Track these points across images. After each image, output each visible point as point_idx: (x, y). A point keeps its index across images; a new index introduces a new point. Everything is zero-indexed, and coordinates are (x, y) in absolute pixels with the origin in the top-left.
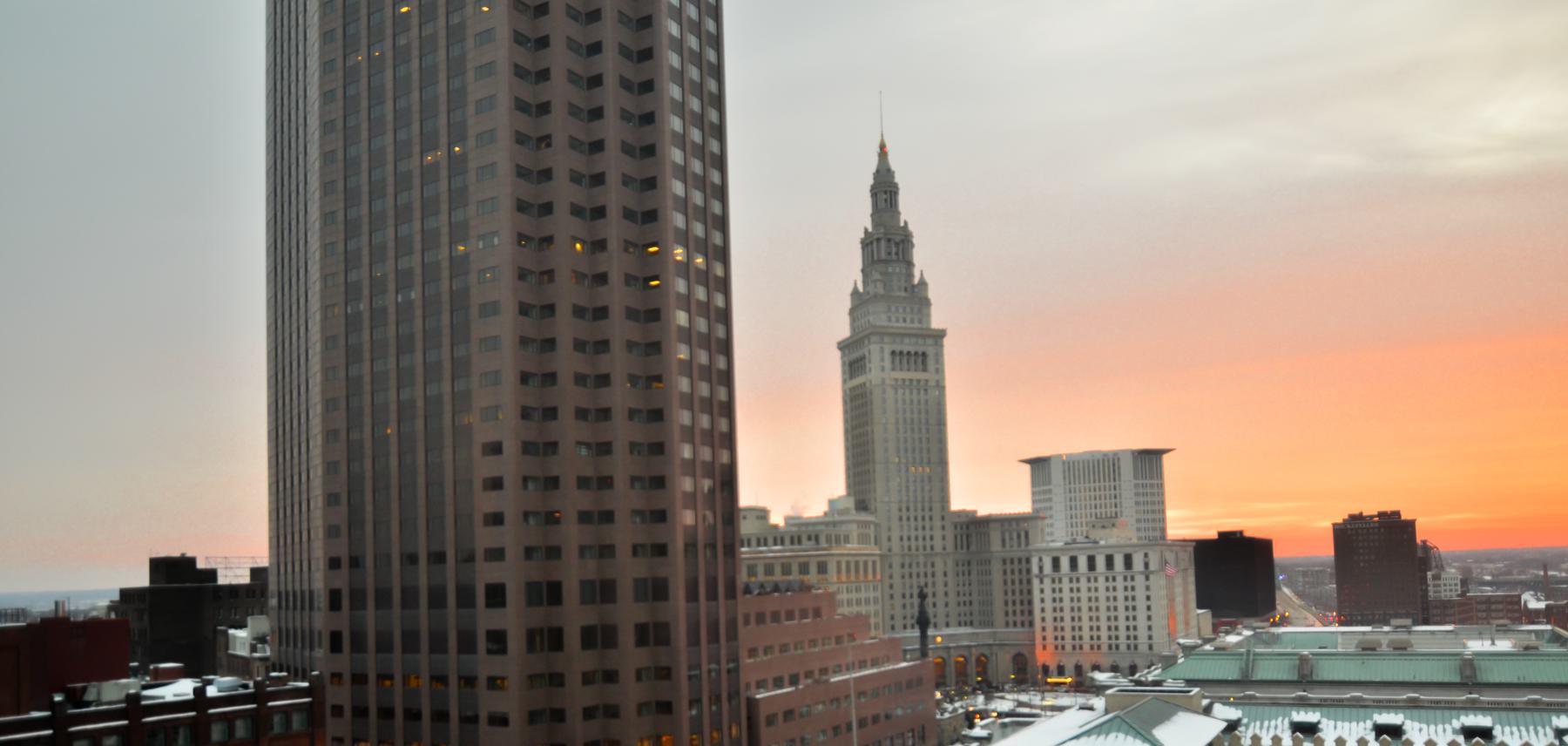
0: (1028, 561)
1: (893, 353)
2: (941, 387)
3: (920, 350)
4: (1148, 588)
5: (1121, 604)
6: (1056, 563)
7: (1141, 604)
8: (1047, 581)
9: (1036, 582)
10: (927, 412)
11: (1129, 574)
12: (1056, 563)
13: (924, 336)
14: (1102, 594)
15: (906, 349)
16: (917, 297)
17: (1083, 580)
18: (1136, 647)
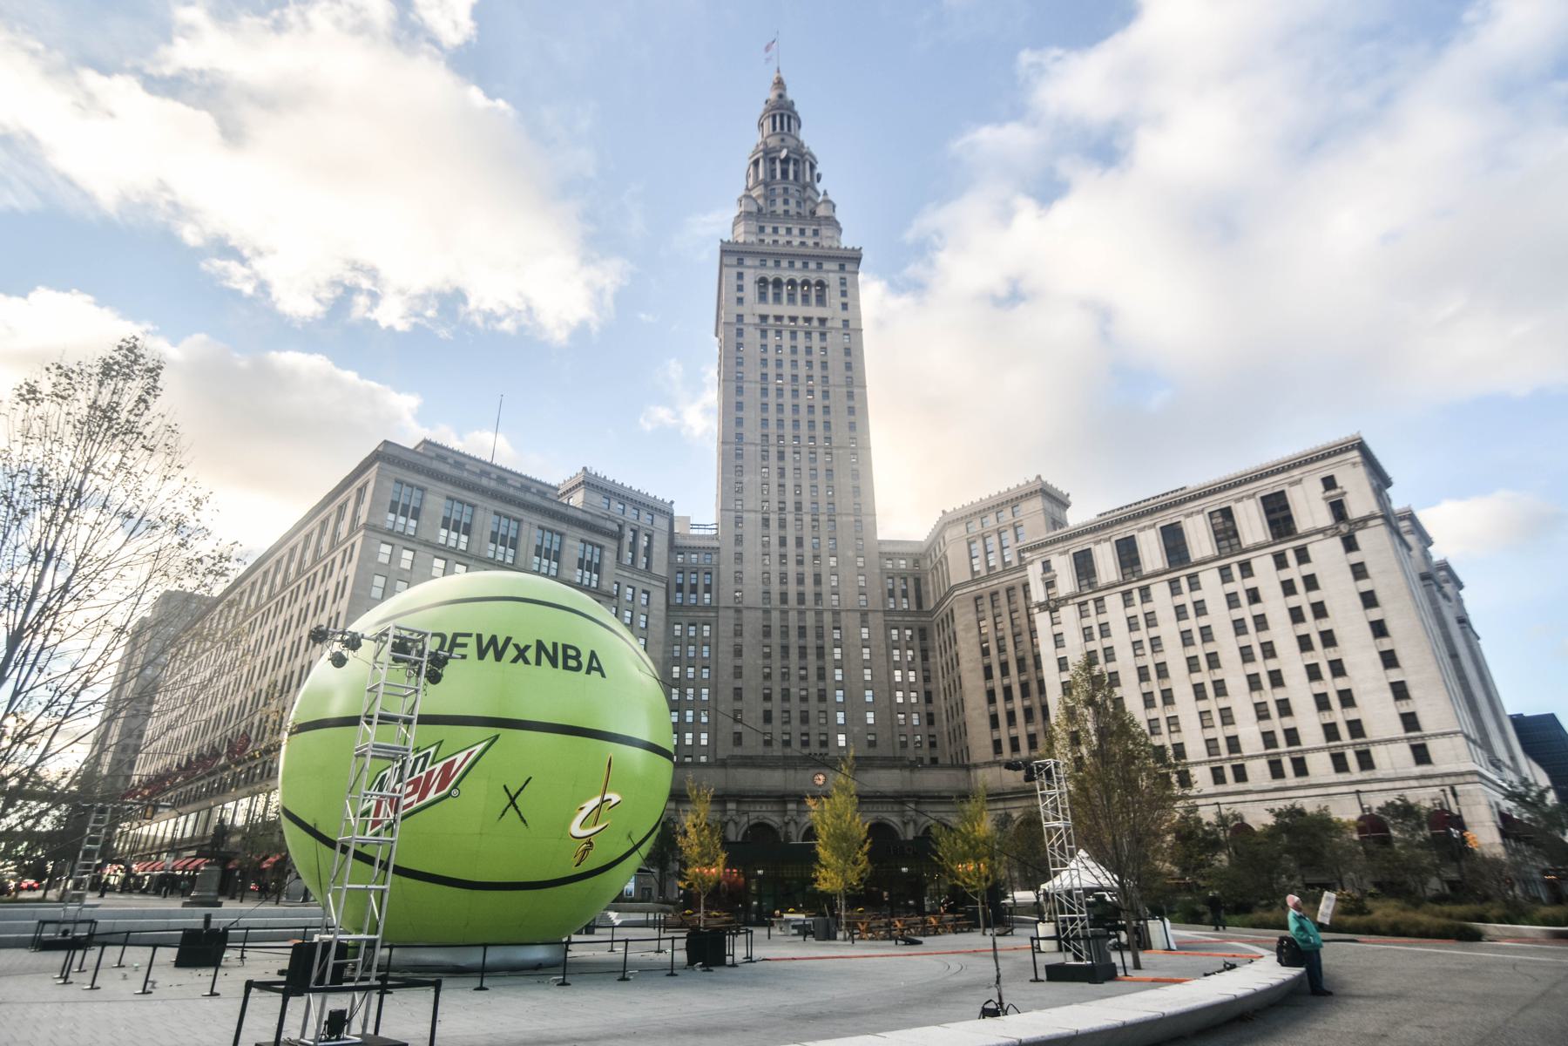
0: (1026, 586)
1: (763, 282)
2: (851, 328)
3: (813, 277)
4: (1359, 571)
5: (1282, 634)
6: (1084, 565)
7: (1349, 621)
8: (1068, 613)
9: (1042, 620)
10: (824, 365)
11: (1288, 547)
12: (1084, 565)
13: (820, 259)
14: (1219, 617)
15: (785, 276)
16: (819, 219)
17: (1160, 590)
18: (1366, 761)
